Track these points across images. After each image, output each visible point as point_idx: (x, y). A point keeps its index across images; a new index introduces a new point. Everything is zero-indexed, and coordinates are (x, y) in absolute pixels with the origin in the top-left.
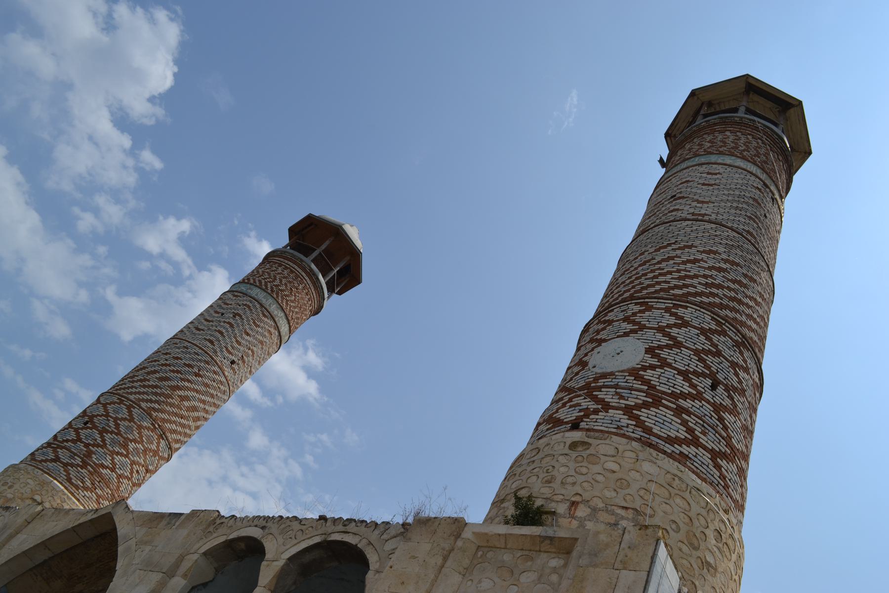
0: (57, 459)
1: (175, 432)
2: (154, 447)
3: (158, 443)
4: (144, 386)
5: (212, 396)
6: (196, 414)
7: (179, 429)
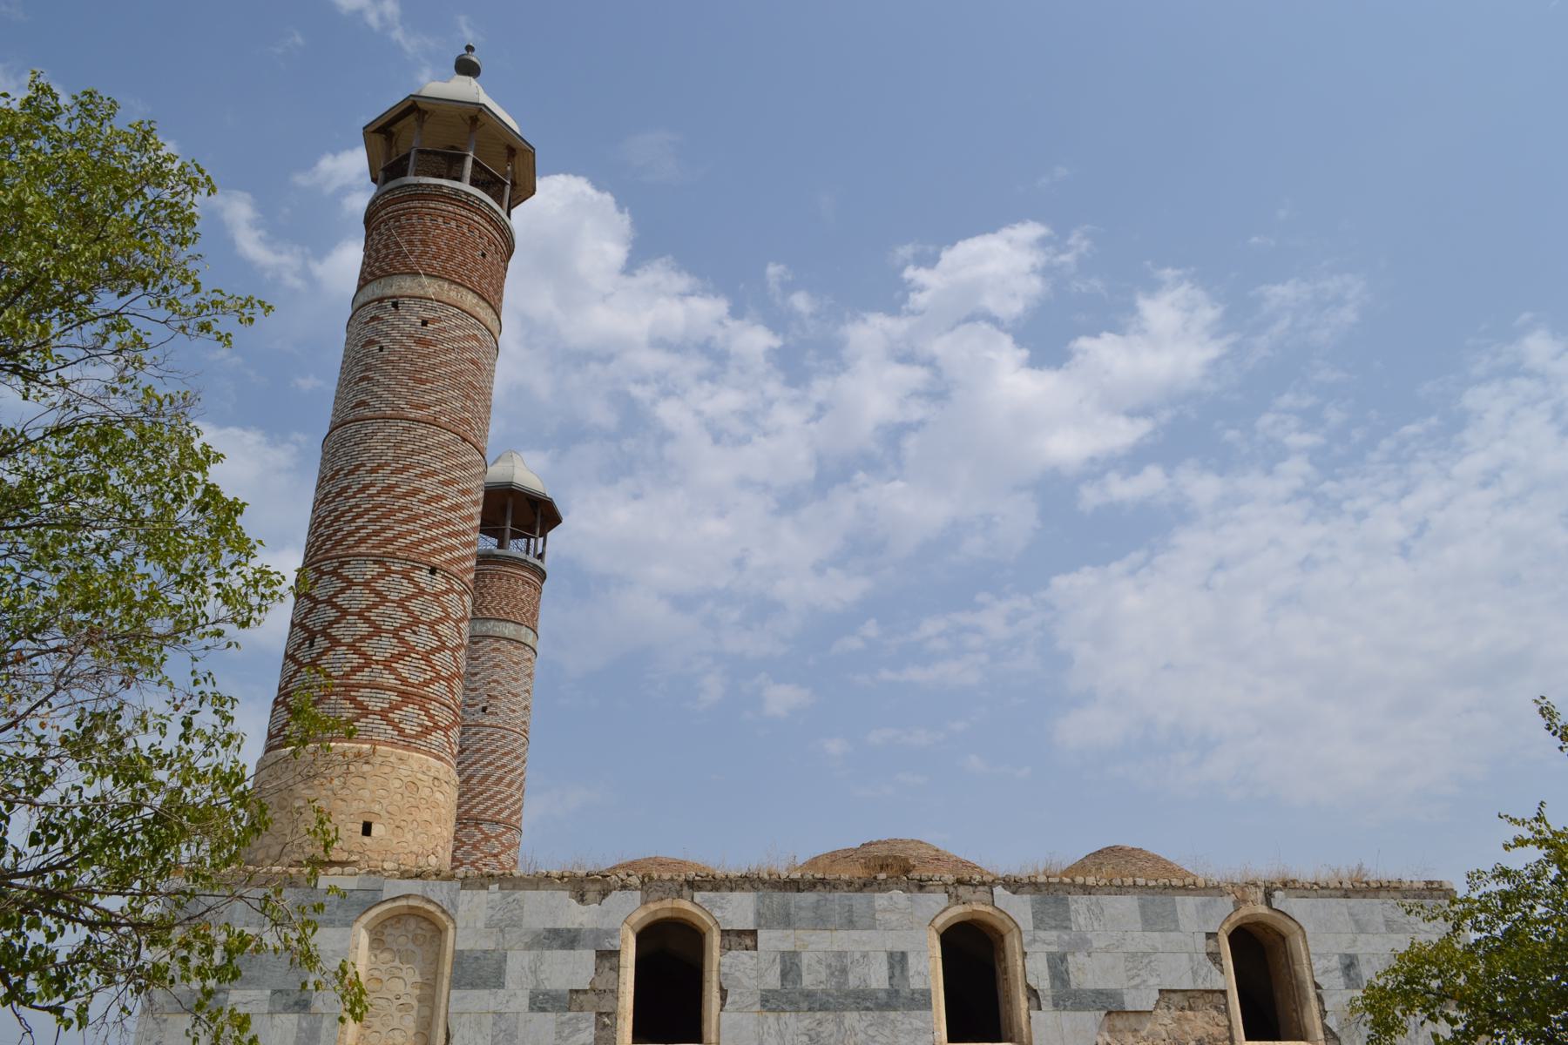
1: (487, 809)
2: (479, 836)
3: (481, 830)
5: (493, 752)
6: (493, 779)
7: (489, 803)
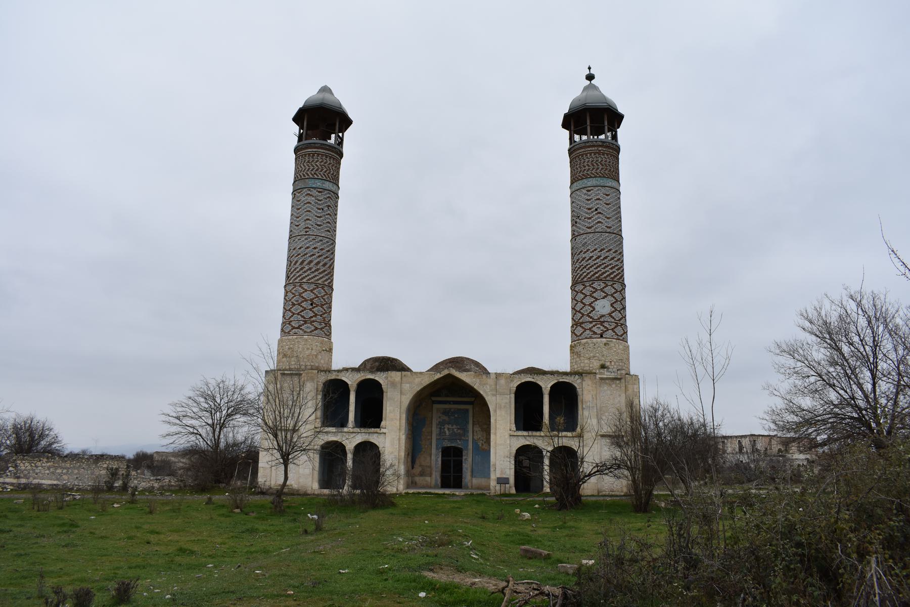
0: (316, 329)
4: (320, 273)
